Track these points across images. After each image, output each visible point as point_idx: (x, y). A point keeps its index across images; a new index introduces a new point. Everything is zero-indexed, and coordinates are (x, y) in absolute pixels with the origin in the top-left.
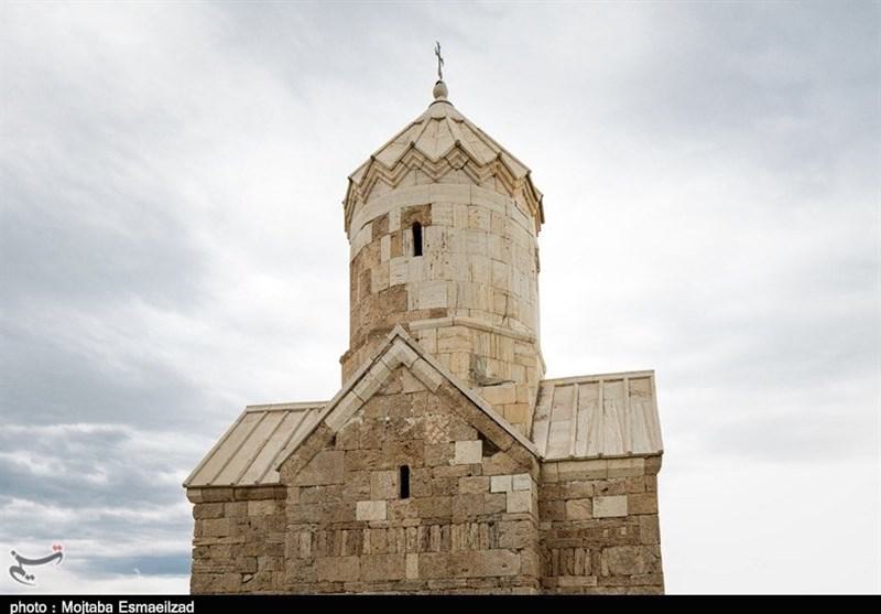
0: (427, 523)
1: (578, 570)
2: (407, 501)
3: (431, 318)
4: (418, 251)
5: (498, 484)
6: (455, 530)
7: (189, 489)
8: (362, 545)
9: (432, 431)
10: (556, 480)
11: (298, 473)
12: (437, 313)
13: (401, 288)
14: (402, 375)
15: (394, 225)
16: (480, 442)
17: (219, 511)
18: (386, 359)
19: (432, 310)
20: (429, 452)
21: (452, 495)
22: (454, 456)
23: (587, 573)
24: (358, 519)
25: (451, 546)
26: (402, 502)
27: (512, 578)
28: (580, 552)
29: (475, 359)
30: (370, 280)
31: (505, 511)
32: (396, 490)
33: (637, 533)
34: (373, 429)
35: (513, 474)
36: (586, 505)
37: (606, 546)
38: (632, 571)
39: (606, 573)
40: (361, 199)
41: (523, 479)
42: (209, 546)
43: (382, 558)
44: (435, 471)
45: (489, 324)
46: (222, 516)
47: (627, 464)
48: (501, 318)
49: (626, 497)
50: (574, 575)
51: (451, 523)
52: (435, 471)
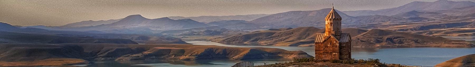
0: (332, 46)
5: (337, 44)
6: (334, 47)
15: (329, 24)
29: (335, 34)
40: (327, 20)
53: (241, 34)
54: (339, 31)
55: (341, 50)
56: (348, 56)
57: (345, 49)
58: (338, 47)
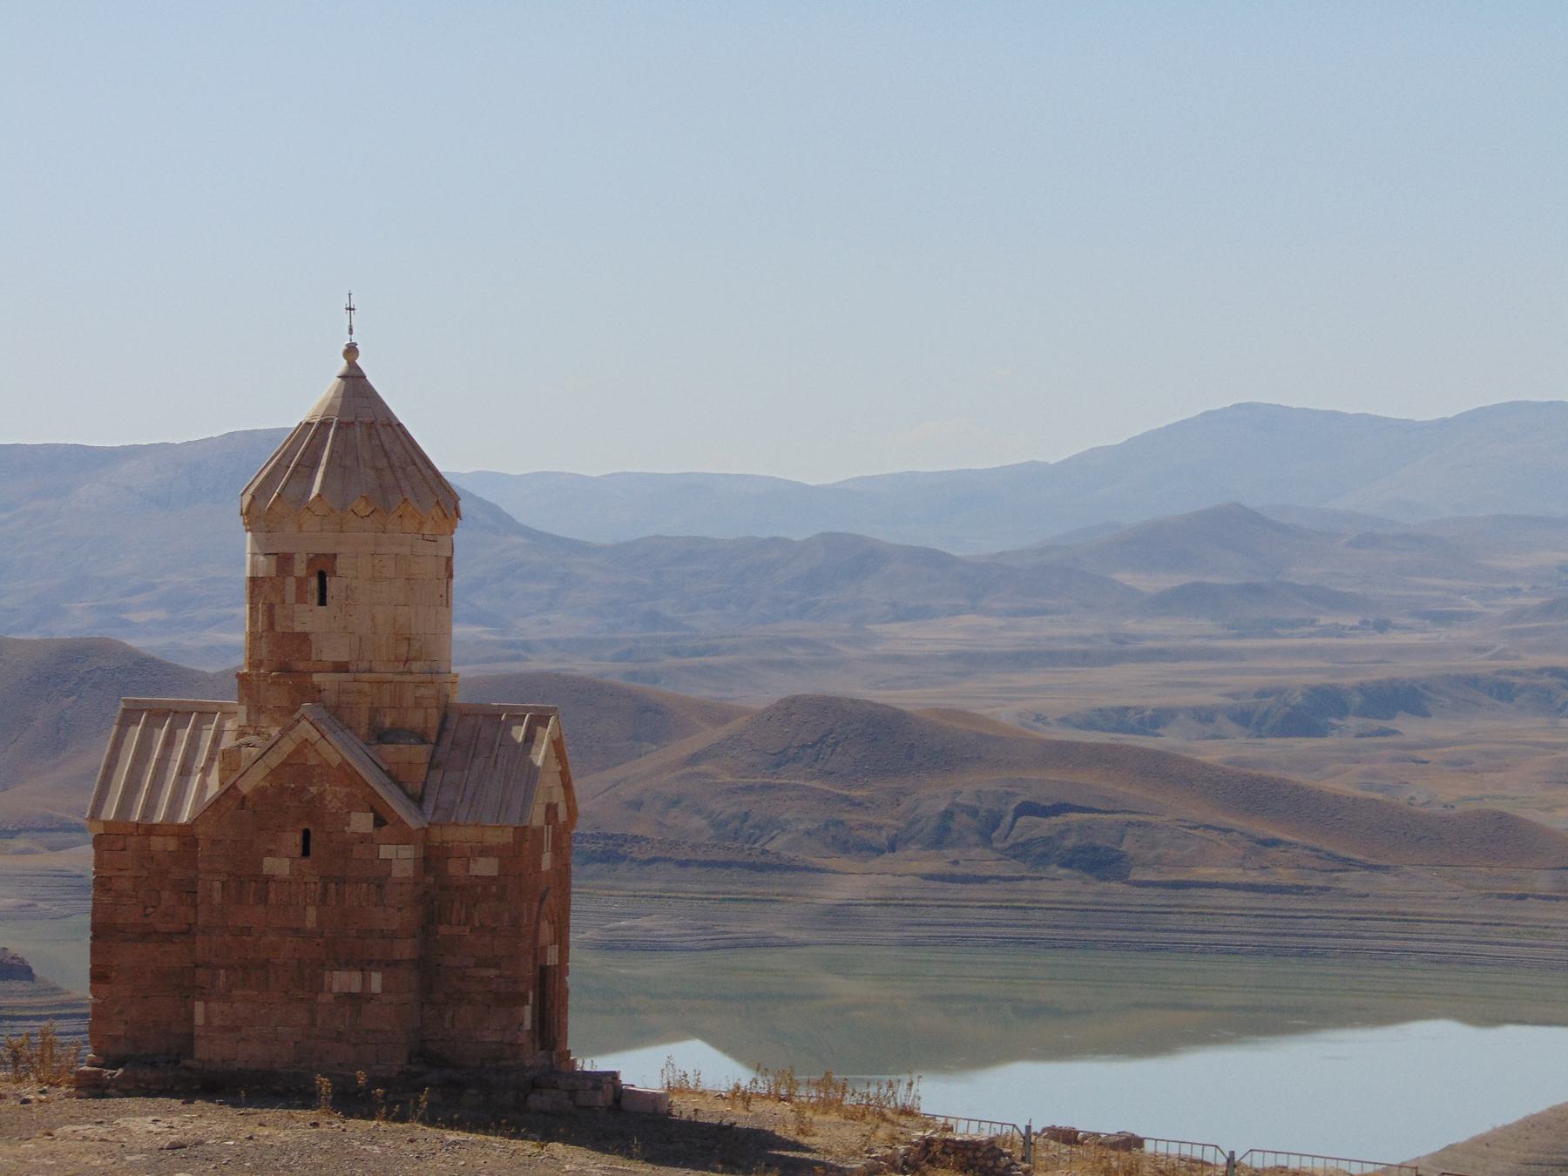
2: (304, 860)
3: (333, 672)
4: (322, 601)
5: (386, 851)
12: (341, 667)
13: (304, 637)
15: (300, 569)
16: (372, 814)
17: (120, 845)
18: (293, 734)
19: (333, 663)
24: (265, 873)
27: (394, 931)
30: (273, 615)
31: (390, 875)
32: (299, 850)
39: (477, 925)
41: (405, 850)
42: (110, 878)
46: (124, 849)
48: (402, 664)
49: (497, 859)
51: (345, 882)
55: (442, 929)
56: (527, 1014)
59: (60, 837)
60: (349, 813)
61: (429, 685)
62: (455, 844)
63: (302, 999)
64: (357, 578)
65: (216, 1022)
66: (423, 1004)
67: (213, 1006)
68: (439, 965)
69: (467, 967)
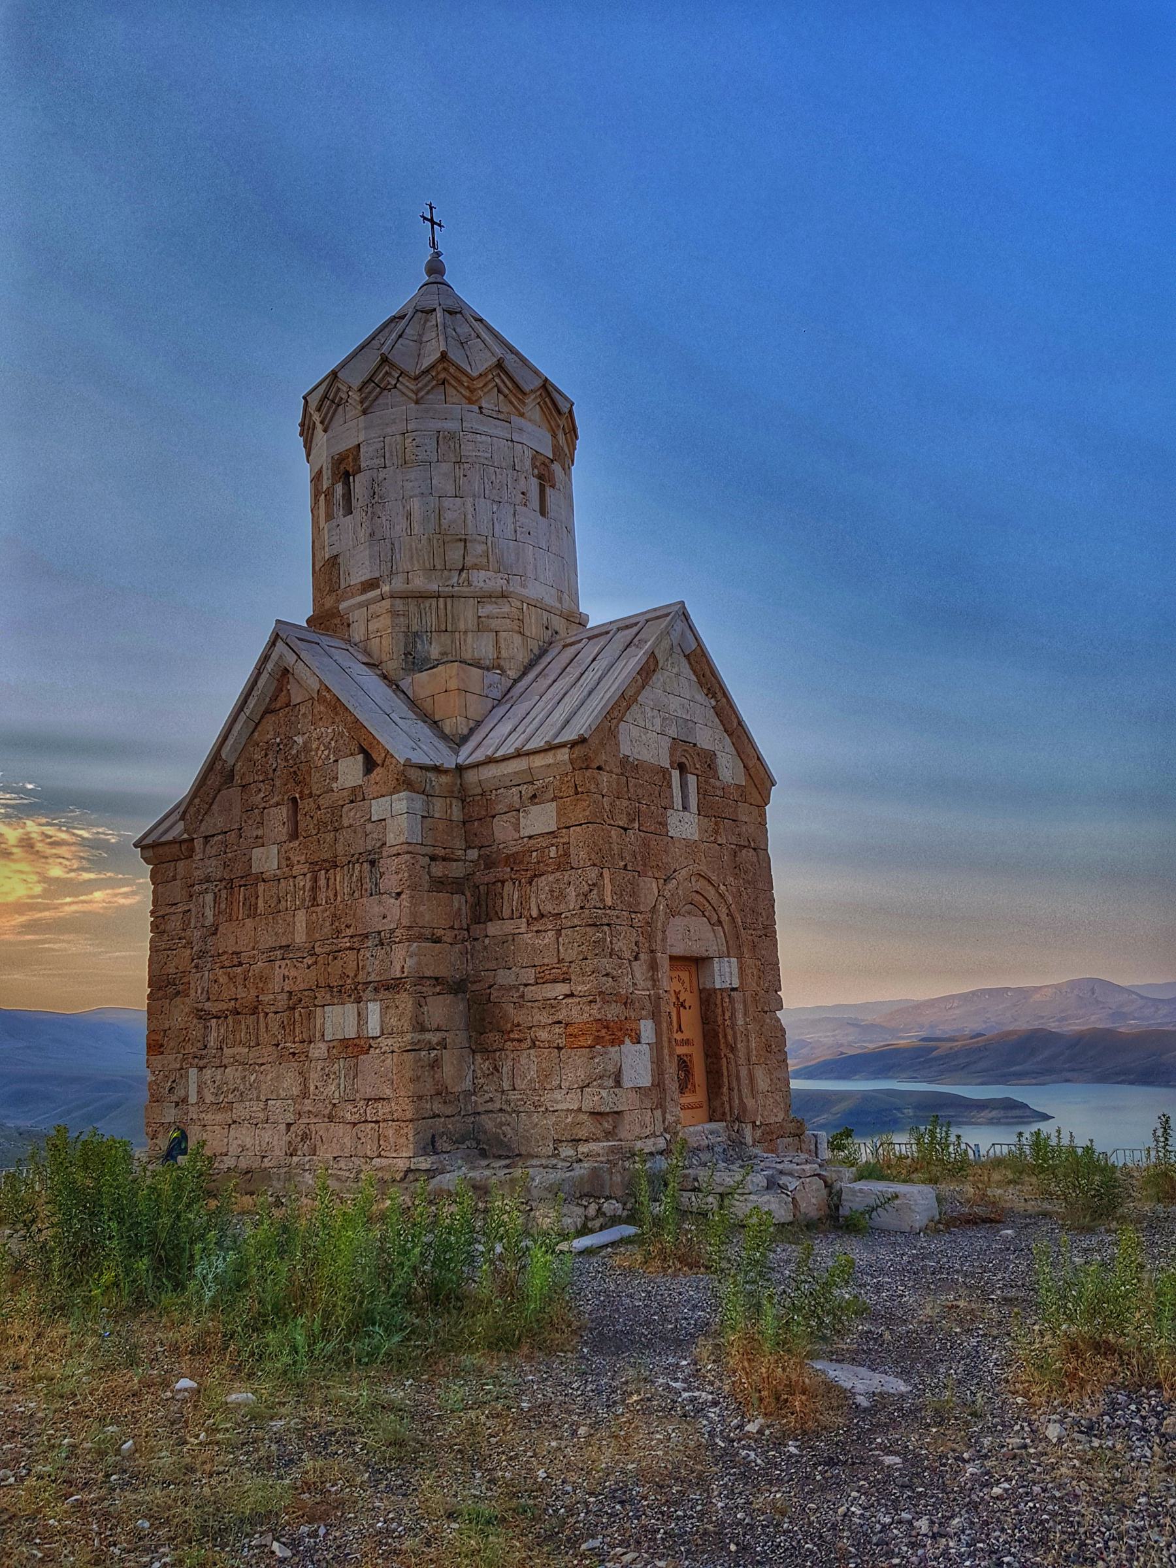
1: (506, 913)
3: (362, 594)
7: (143, 848)
8: (257, 904)
9: (318, 749)
10: (479, 791)
11: (202, 821)
12: (371, 585)
14: (288, 682)
16: (360, 757)
18: (270, 666)
19: (362, 583)
20: (316, 776)
21: (336, 830)
22: (337, 778)
23: (516, 914)
25: (336, 895)
26: (291, 845)
28: (508, 886)
29: (412, 637)
32: (282, 832)
33: (567, 854)
34: (266, 755)
35: (392, 794)
36: (513, 820)
37: (535, 876)
38: (562, 907)
39: (535, 913)
42: (163, 917)
43: (273, 918)
44: (321, 801)
45: (434, 587)
47: (549, 759)
48: (455, 574)
49: (555, 803)
50: (503, 919)
52: (321, 801)
53: (842, 1053)
54: (482, 580)
55: (493, 929)
57: (562, 896)
58: (394, 873)
59: (1034, 1075)
60: (336, 761)
61: (501, 599)
62: (499, 791)
63: (294, 1054)
64: (385, 467)
65: (209, 1098)
66: (474, 1052)
67: (208, 1072)
68: (490, 987)
69: (526, 985)
